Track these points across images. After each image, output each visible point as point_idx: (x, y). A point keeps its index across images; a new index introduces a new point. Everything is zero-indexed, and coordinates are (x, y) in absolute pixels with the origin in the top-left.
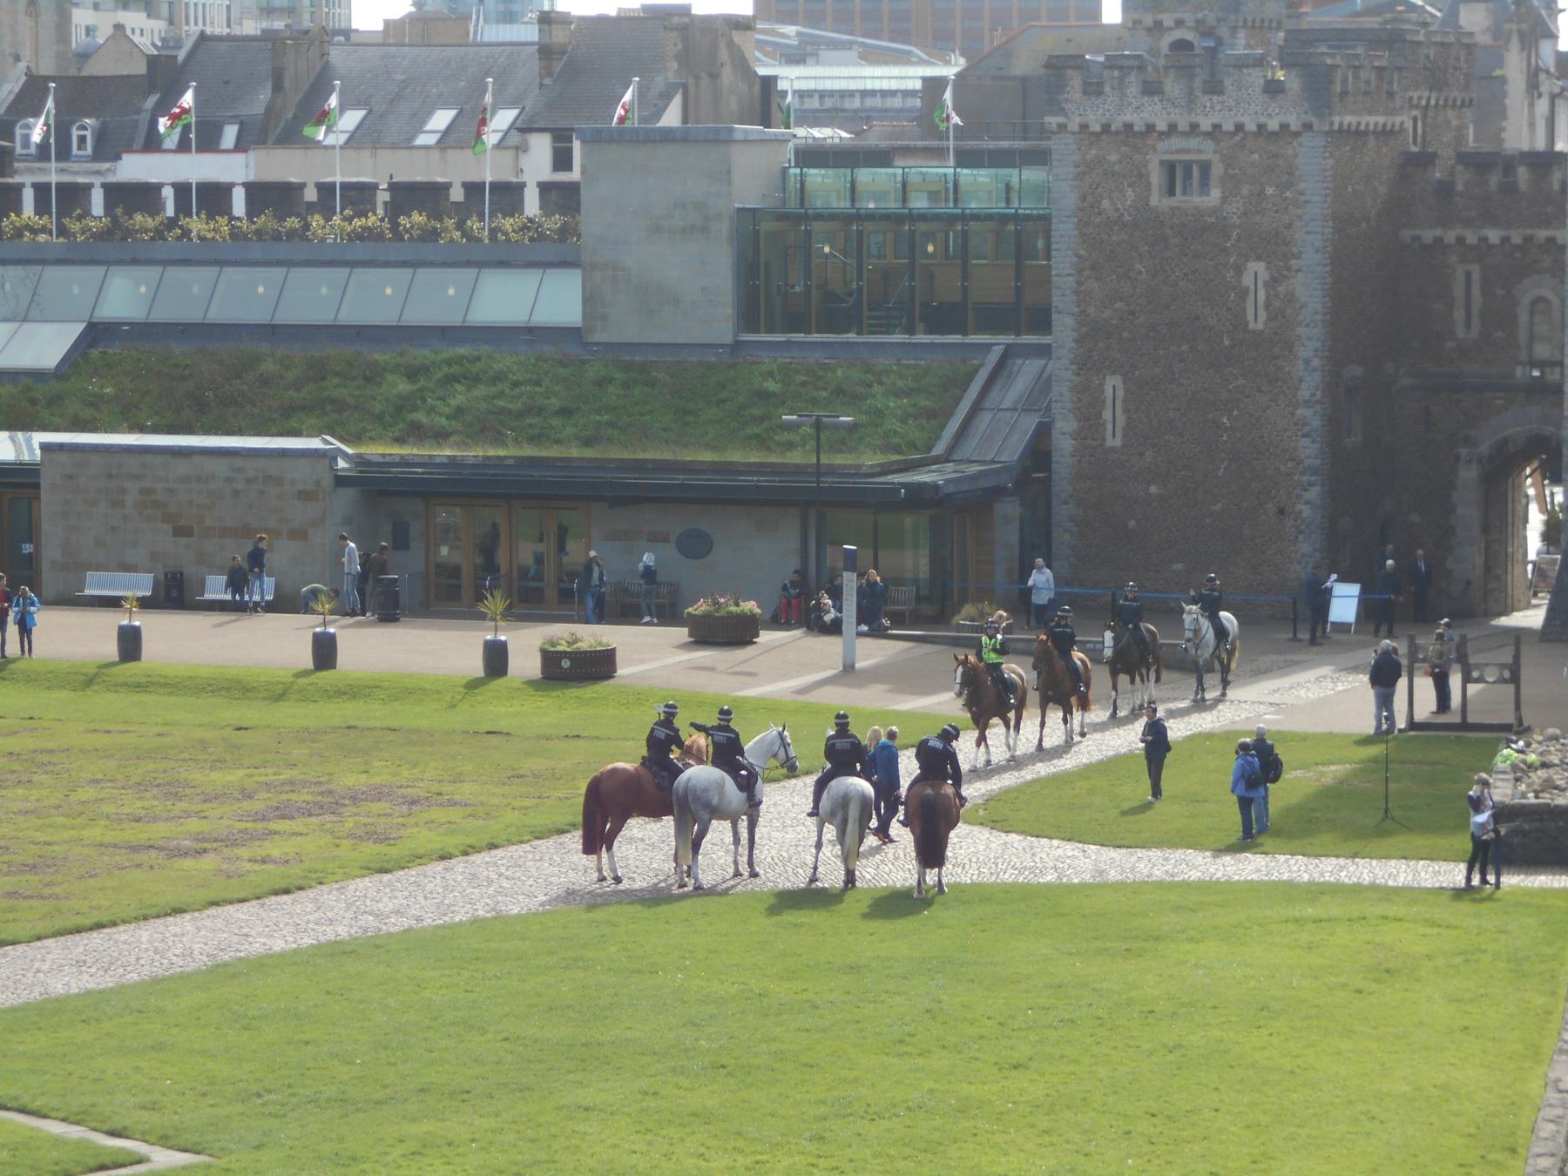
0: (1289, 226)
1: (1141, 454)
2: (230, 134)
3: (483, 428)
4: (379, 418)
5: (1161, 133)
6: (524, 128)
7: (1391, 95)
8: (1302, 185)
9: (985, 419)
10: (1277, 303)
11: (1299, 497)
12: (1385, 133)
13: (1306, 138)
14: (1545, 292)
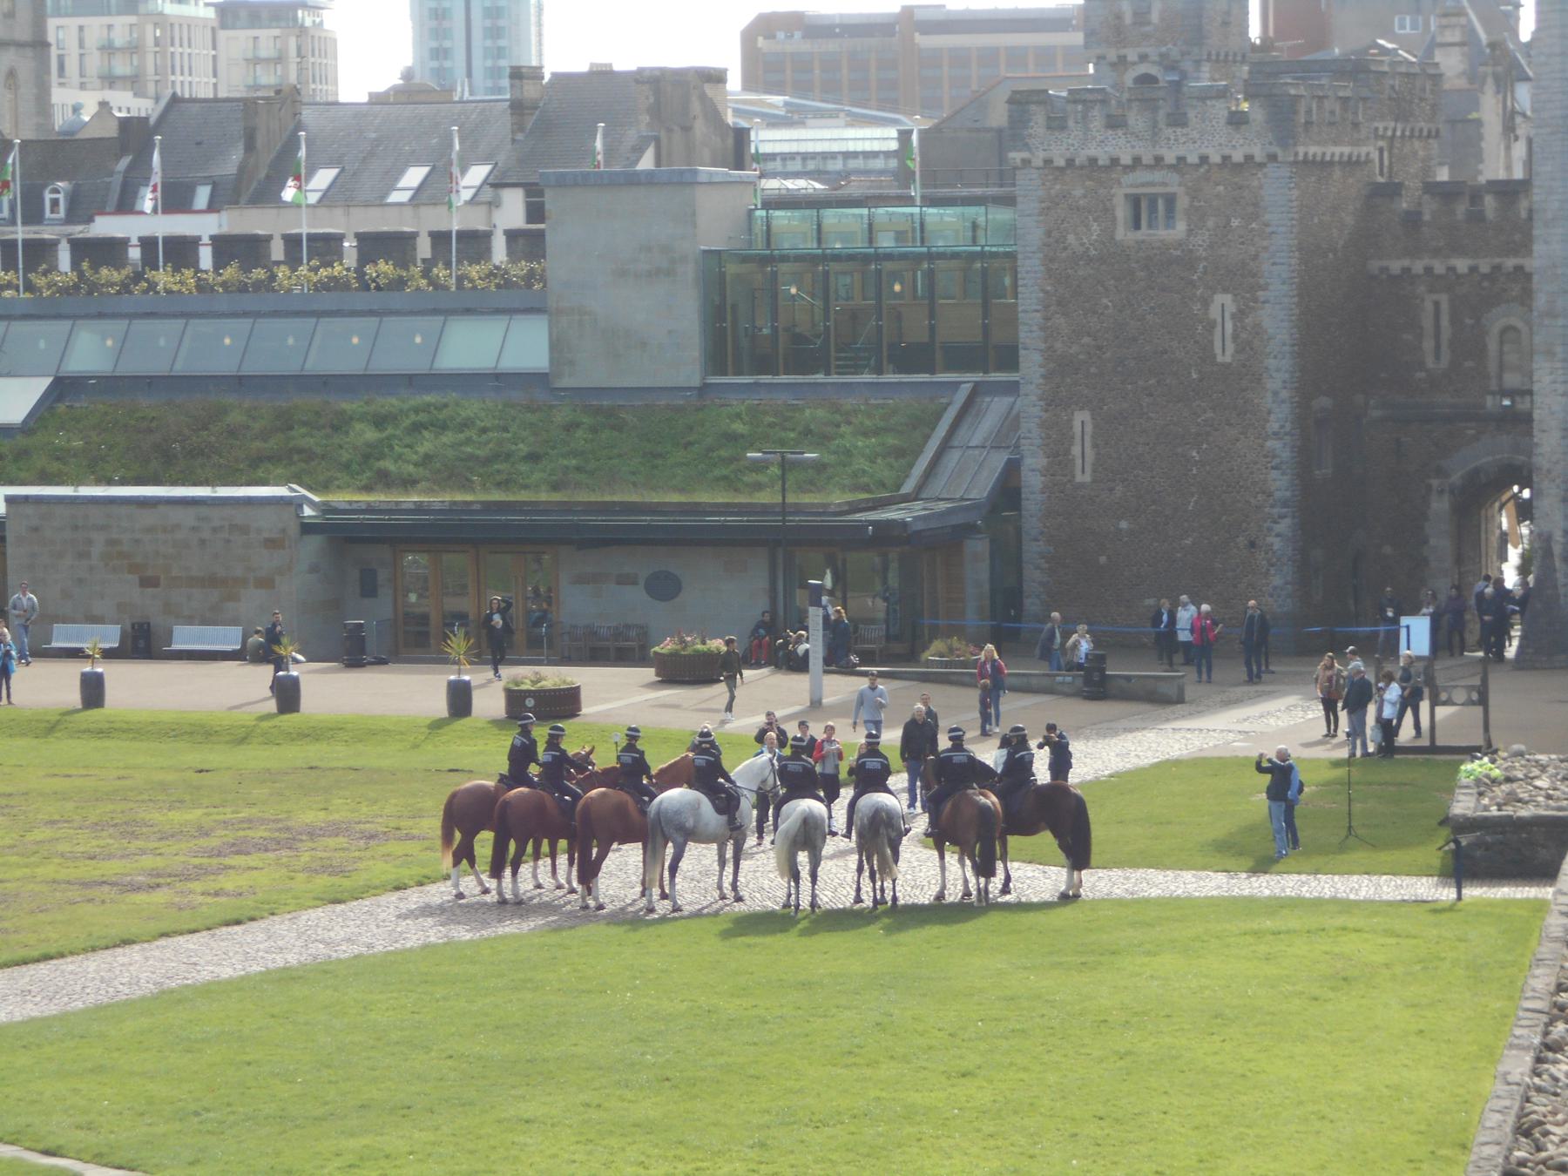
0: (1255, 257)
1: (1111, 490)
2: (202, 196)
3: (451, 475)
4: (347, 466)
5: (1126, 167)
6: (496, 183)
7: (1356, 125)
8: (1267, 217)
9: (953, 458)
10: (1244, 335)
11: (1270, 529)
12: (1351, 164)
13: (1271, 169)
14: (1515, 321)
